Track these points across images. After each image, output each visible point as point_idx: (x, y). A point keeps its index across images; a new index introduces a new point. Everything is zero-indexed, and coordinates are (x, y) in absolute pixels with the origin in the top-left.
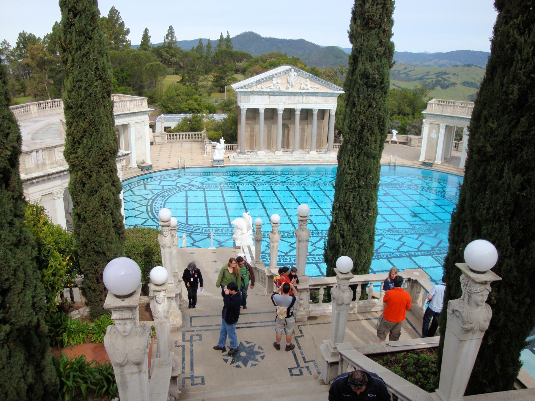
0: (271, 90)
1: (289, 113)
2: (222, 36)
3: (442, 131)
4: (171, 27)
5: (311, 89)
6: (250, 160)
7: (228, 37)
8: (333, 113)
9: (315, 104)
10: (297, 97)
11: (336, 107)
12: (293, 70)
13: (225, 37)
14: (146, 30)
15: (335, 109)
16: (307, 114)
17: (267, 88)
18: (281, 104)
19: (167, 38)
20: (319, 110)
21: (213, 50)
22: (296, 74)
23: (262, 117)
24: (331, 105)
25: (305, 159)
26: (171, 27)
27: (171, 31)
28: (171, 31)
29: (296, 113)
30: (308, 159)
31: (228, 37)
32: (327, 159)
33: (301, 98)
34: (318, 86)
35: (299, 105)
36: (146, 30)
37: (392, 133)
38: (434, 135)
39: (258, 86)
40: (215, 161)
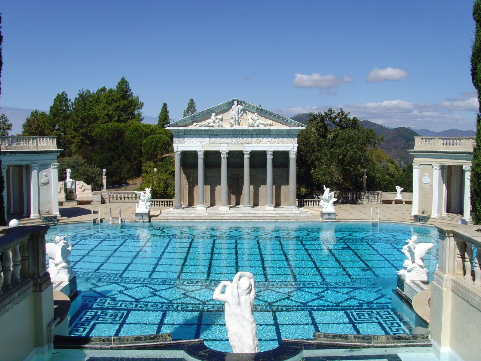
0: (210, 128)
1: (235, 158)
3: (437, 173)
4: (192, 101)
5: (261, 125)
6: (185, 215)
8: (293, 156)
11: (296, 148)
12: (236, 102)
15: (296, 150)
16: (258, 158)
17: (204, 125)
18: (224, 146)
22: (241, 107)
24: (291, 146)
25: (256, 215)
26: (192, 101)
29: (245, 156)
30: (260, 215)
32: (286, 215)
34: (270, 122)
35: (248, 146)
37: (396, 191)
38: (426, 180)
39: (195, 124)
40: (137, 215)
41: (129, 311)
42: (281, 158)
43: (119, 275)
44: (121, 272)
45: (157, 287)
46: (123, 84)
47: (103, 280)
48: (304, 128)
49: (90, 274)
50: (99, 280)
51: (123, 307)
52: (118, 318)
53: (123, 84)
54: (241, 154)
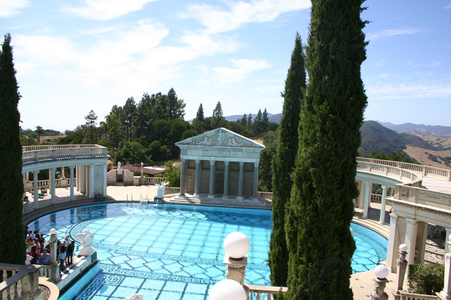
2: (260, 111)
4: (219, 102)
7: (265, 111)
8: (257, 166)
9: (241, 158)
10: (225, 152)
12: (220, 131)
13: (262, 112)
14: (201, 105)
15: (258, 161)
19: (216, 110)
20: (245, 163)
21: (253, 120)
23: (197, 167)
24: (255, 160)
27: (219, 107)
28: (219, 107)
29: (226, 165)
31: (265, 111)
33: (229, 153)
36: (201, 105)
41: (125, 276)
42: (248, 167)
43: (129, 248)
44: (131, 246)
45: (148, 260)
46: (172, 91)
47: (118, 252)
48: (264, 149)
49: (113, 246)
50: (116, 253)
51: (123, 274)
52: (117, 281)
53: (172, 91)
54: (223, 163)
